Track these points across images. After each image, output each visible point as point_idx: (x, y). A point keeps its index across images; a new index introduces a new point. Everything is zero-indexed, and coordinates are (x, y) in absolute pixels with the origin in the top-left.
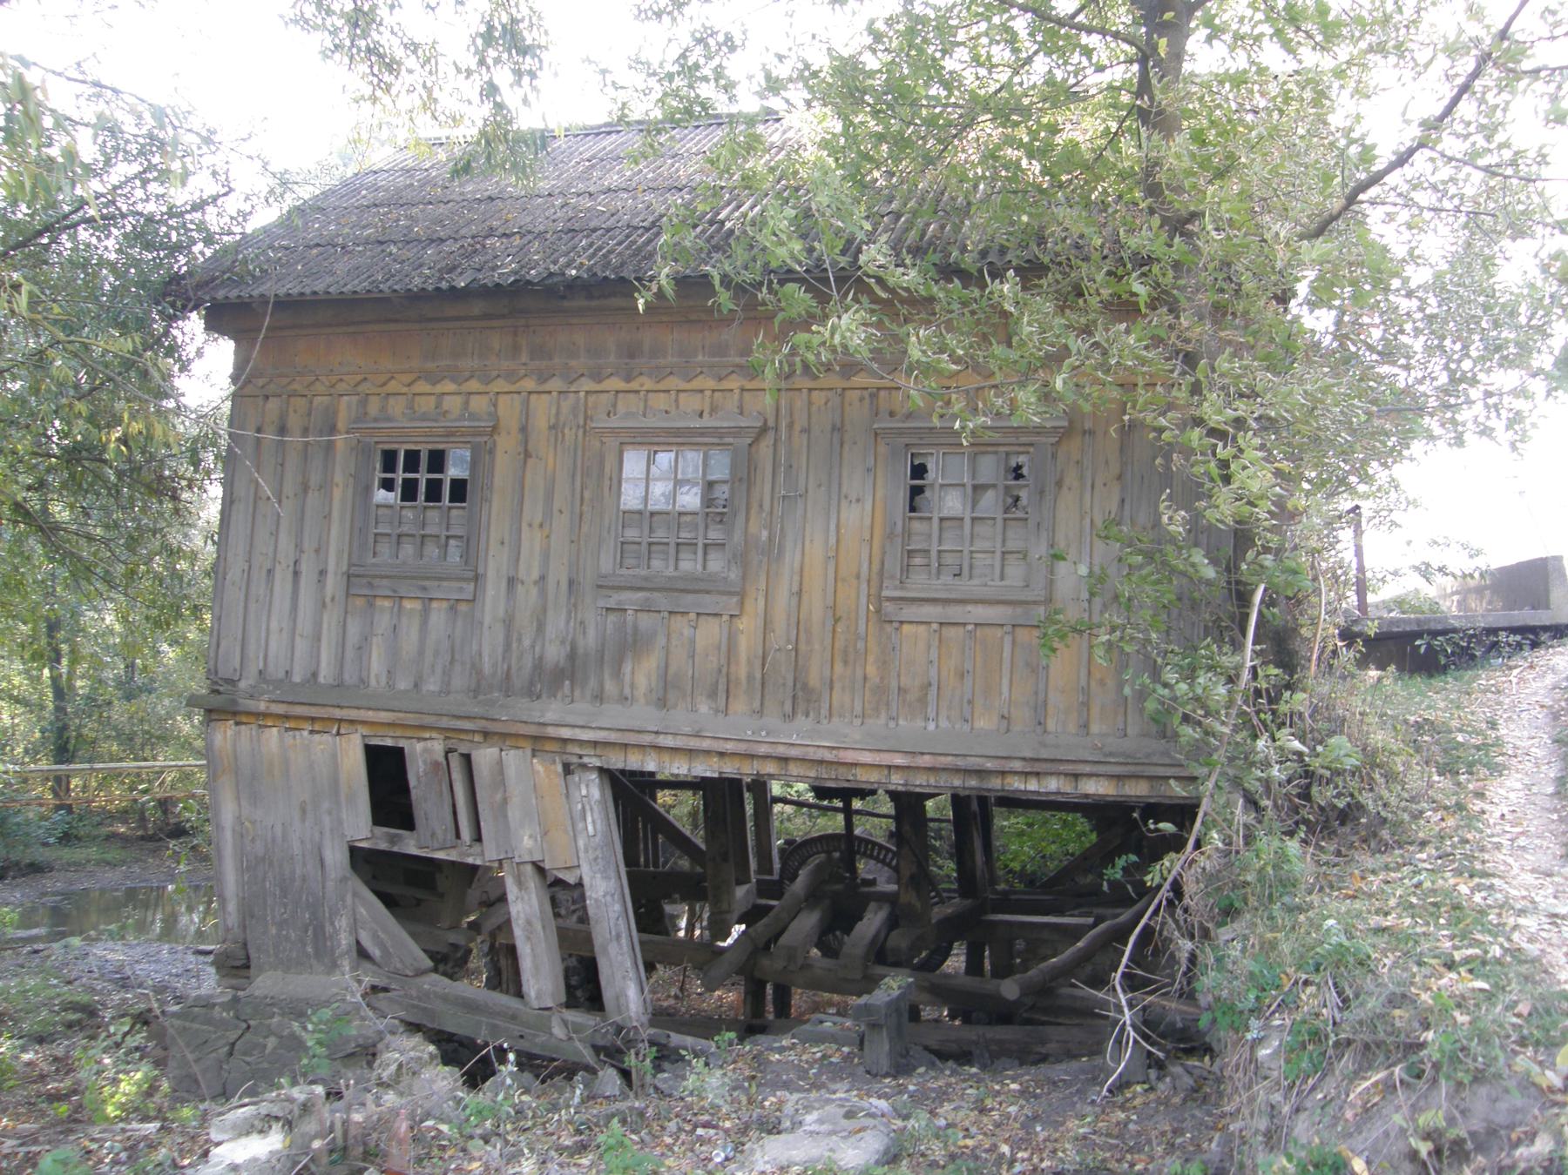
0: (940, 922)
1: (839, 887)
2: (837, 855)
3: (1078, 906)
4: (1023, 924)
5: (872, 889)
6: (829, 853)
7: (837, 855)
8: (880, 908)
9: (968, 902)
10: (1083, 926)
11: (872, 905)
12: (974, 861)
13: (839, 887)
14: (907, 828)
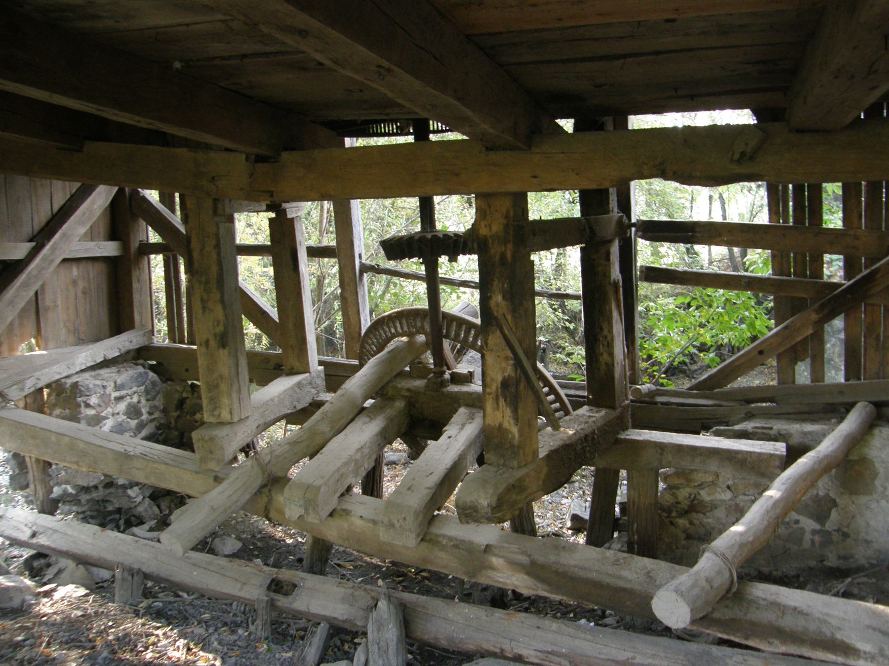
0: (549, 457)
1: (419, 383)
2: (421, 338)
3: (750, 416)
4: (680, 449)
5: (465, 389)
6: (411, 335)
7: (421, 338)
8: (472, 418)
9: (603, 412)
10: (771, 455)
11: (462, 410)
12: (611, 354)
13: (419, 383)
14: (498, 299)
